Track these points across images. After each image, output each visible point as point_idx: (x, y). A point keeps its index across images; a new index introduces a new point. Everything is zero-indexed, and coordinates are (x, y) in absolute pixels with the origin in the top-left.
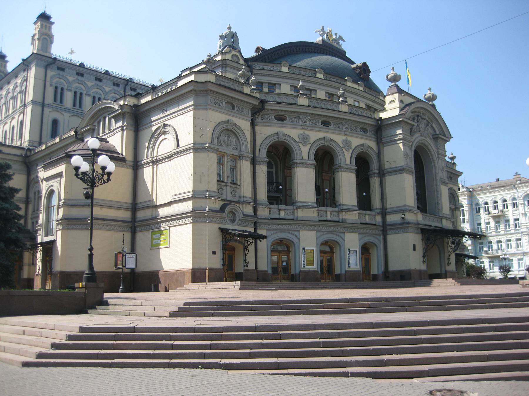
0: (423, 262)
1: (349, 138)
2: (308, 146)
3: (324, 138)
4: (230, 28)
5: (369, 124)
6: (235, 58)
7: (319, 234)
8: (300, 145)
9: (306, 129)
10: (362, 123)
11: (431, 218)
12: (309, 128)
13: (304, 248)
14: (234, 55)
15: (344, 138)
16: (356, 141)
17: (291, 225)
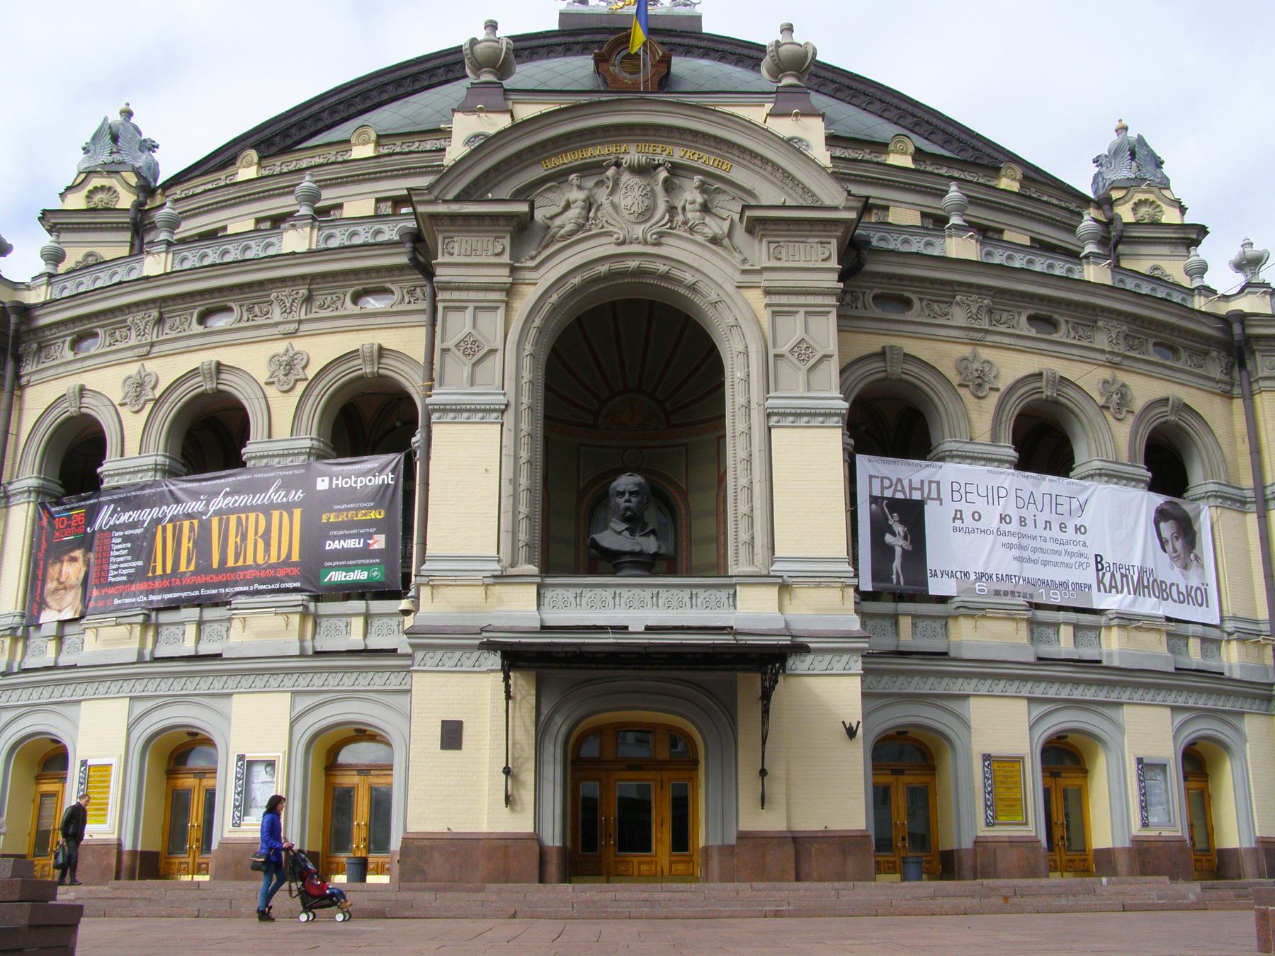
0: (509, 800)
1: (299, 344)
2: (149, 406)
3: (194, 372)
4: (128, 114)
5: (390, 270)
6: (98, 197)
7: (141, 707)
8: (125, 413)
9: (146, 357)
10: (356, 273)
11: (626, 593)
12: (155, 349)
13: (84, 763)
14: (96, 190)
15: (280, 347)
16: (326, 347)
17: (56, 683)
